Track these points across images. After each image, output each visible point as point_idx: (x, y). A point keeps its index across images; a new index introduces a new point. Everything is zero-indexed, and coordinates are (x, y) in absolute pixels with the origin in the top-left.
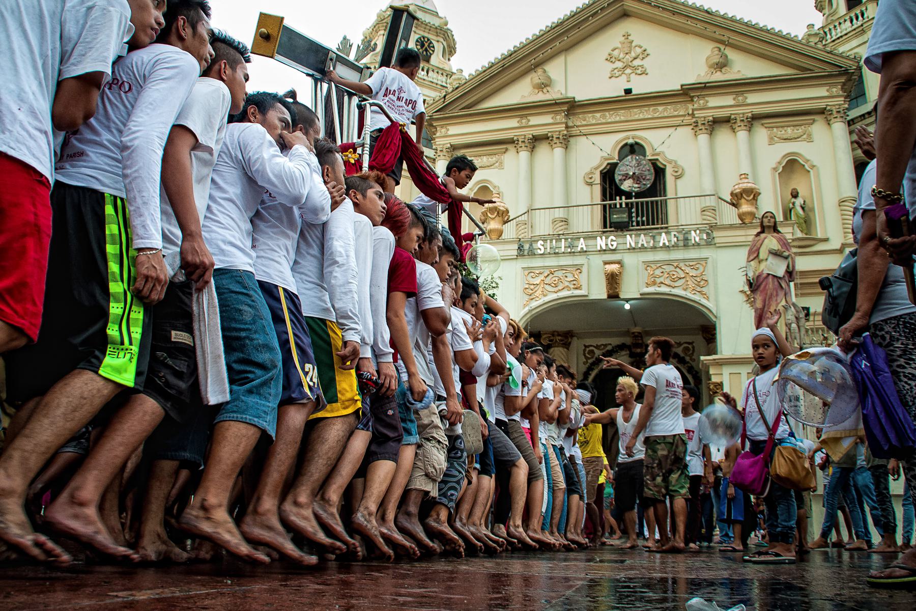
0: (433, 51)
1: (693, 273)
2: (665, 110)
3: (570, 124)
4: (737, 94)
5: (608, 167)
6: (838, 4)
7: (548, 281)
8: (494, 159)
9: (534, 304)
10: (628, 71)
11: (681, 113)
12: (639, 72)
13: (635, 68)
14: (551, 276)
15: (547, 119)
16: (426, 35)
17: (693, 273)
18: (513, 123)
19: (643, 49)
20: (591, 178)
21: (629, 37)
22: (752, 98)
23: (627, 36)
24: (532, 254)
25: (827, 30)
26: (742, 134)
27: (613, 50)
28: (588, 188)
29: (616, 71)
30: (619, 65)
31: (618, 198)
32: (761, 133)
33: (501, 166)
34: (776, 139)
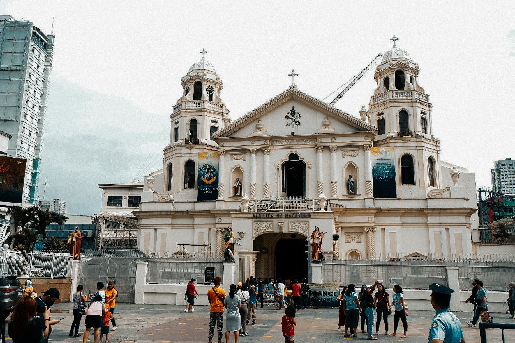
0: (214, 92)
2: (306, 141)
3: (271, 144)
4: (333, 138)
6: (381, 84)
7: (261, 226)
8: (241, 156)
9: (257, 233)
10: (293, 123)
11: (312, 143)
12: (297, 124)
13: (296, 122)
15: (262, 143)
16: (211, 85)
17: (304, 226)
18: (249, 143)
19: (299, 114)
22: (338, 140)
23: (293, 108)
24: (257, 217)
25: (374, 98)
26: (334, 154)
27: (288, 114)
28: (277, 171)
29: (288, 123)
30: (289, 120)
32: (340, 153)
33: (244, 160)
34: (345, 155)
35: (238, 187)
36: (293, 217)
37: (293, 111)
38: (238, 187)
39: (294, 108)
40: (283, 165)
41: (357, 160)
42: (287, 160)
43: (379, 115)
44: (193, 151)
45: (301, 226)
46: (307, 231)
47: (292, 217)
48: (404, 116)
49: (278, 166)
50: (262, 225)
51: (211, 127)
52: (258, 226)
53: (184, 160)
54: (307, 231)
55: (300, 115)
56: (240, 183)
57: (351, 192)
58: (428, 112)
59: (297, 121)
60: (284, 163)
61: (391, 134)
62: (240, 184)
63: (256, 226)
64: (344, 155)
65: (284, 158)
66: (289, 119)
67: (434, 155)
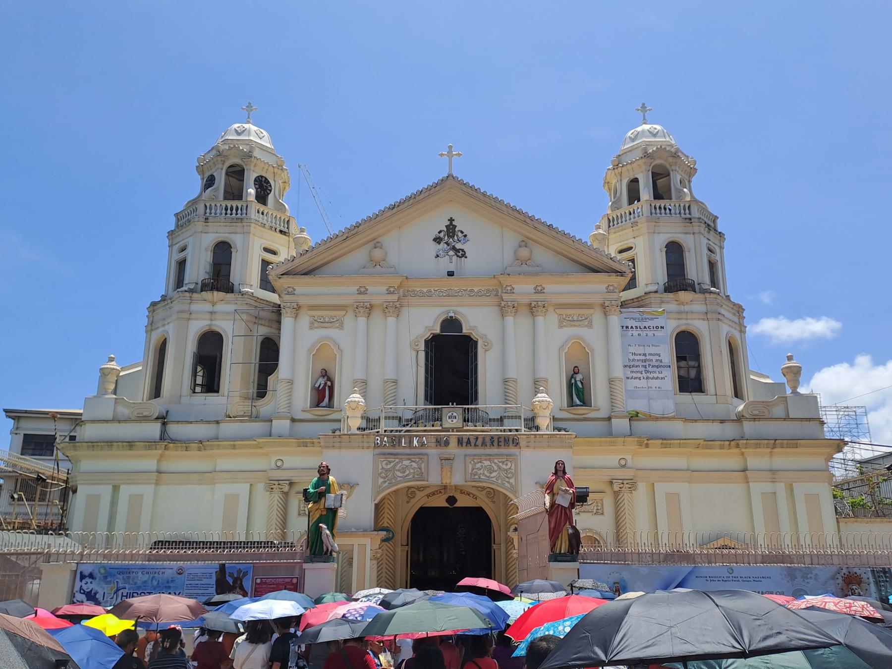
1: (504, 467)
5: (432, 336)
10: (451, 253)
14: (400, 464)
17: (504, 467)
19: (464, 234)
20: (417, 345)
21: (453, 222)
23: (451, 220)
27: (440, 232)
29: (441, 252)
30: (443, 245)
31: (450, 403)
33: (341, 327)
35: (324, 388)
36: (476, 445)
37: (451, 227)
38: (324, 388)
39: (454, 220)
40: (426, 342)
41: (592, 336)
42: (438, 331)
43: (621, 252)
44: (220, 307)
45: (496, 468)
46: (512, 481)
47: (473, 444)
48: (674, 251)
49: (416, 344)
50: (399, 465)
51: (263, 260)
52: (389, 466)
53: (197, 327)
54: (512, 481)
55: (465, 236)
56: (329, 379)
57: (578, 402)
58: (717, 249)
59: (460, 249)
60: (430, 338)
61: (653, 288)
62: (329, 383)
63: (383, 468)
64: (560, 322)
65: (430, 324)
66: (442, 243)
67: (737, 335)
